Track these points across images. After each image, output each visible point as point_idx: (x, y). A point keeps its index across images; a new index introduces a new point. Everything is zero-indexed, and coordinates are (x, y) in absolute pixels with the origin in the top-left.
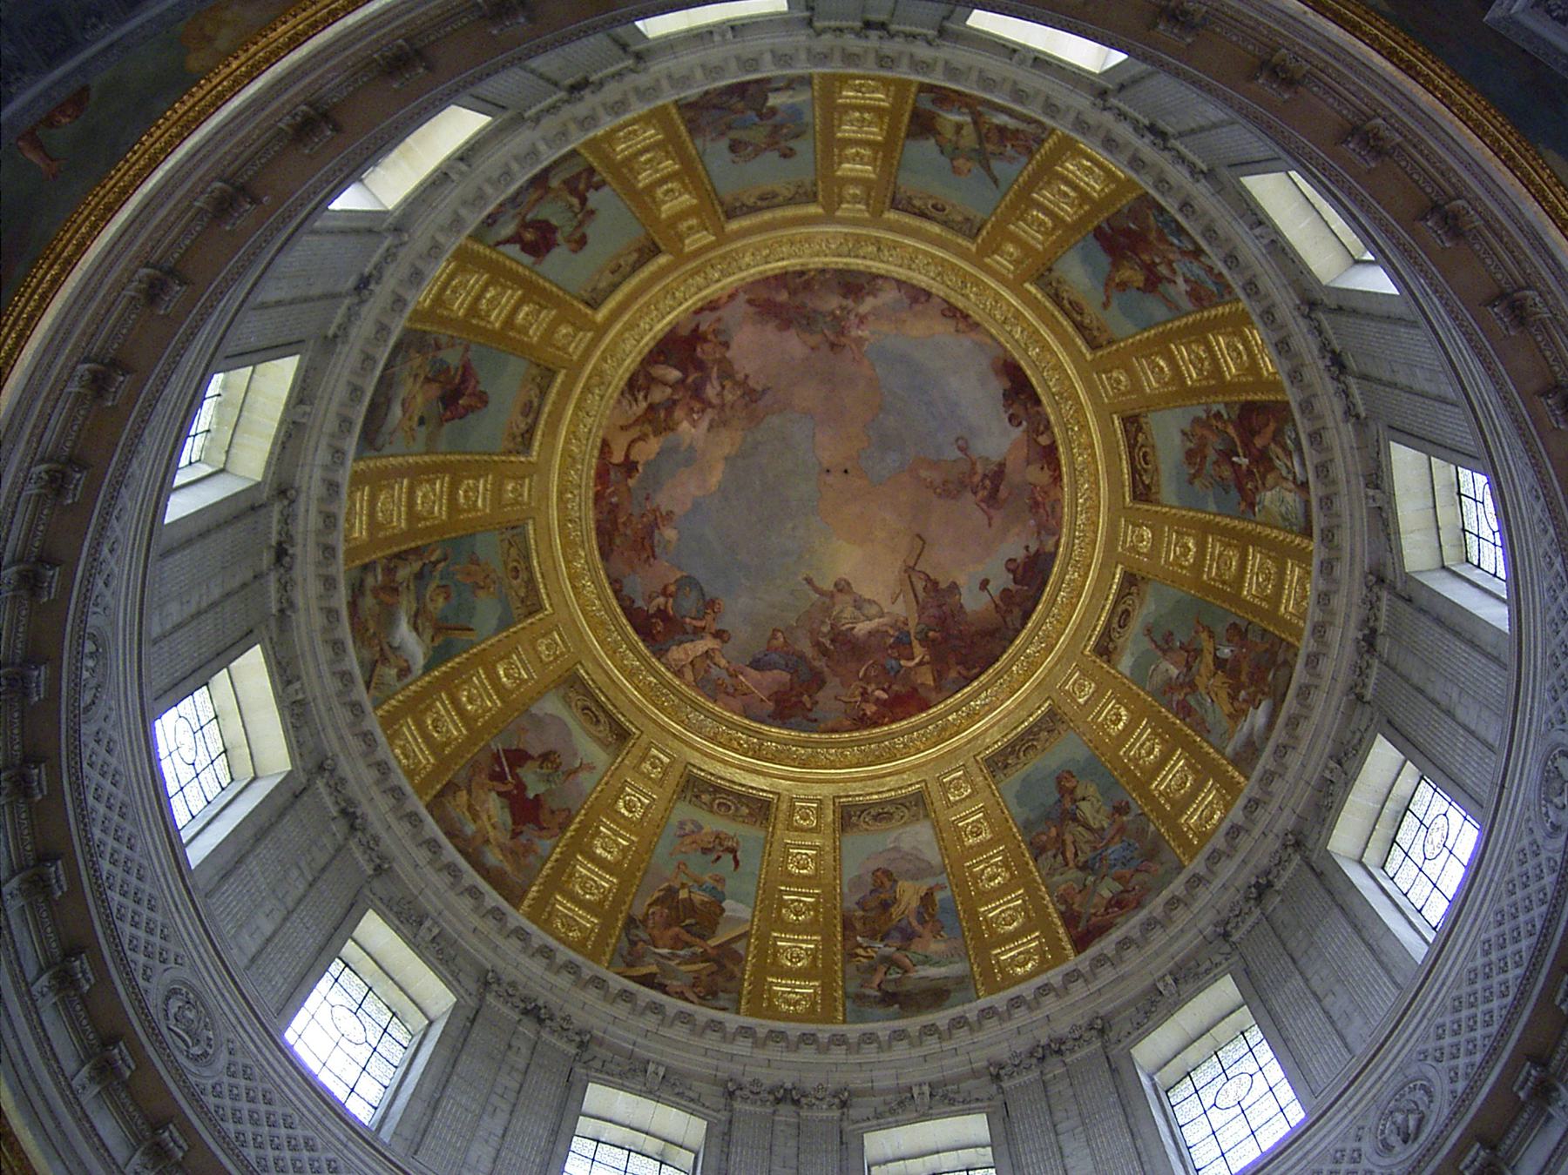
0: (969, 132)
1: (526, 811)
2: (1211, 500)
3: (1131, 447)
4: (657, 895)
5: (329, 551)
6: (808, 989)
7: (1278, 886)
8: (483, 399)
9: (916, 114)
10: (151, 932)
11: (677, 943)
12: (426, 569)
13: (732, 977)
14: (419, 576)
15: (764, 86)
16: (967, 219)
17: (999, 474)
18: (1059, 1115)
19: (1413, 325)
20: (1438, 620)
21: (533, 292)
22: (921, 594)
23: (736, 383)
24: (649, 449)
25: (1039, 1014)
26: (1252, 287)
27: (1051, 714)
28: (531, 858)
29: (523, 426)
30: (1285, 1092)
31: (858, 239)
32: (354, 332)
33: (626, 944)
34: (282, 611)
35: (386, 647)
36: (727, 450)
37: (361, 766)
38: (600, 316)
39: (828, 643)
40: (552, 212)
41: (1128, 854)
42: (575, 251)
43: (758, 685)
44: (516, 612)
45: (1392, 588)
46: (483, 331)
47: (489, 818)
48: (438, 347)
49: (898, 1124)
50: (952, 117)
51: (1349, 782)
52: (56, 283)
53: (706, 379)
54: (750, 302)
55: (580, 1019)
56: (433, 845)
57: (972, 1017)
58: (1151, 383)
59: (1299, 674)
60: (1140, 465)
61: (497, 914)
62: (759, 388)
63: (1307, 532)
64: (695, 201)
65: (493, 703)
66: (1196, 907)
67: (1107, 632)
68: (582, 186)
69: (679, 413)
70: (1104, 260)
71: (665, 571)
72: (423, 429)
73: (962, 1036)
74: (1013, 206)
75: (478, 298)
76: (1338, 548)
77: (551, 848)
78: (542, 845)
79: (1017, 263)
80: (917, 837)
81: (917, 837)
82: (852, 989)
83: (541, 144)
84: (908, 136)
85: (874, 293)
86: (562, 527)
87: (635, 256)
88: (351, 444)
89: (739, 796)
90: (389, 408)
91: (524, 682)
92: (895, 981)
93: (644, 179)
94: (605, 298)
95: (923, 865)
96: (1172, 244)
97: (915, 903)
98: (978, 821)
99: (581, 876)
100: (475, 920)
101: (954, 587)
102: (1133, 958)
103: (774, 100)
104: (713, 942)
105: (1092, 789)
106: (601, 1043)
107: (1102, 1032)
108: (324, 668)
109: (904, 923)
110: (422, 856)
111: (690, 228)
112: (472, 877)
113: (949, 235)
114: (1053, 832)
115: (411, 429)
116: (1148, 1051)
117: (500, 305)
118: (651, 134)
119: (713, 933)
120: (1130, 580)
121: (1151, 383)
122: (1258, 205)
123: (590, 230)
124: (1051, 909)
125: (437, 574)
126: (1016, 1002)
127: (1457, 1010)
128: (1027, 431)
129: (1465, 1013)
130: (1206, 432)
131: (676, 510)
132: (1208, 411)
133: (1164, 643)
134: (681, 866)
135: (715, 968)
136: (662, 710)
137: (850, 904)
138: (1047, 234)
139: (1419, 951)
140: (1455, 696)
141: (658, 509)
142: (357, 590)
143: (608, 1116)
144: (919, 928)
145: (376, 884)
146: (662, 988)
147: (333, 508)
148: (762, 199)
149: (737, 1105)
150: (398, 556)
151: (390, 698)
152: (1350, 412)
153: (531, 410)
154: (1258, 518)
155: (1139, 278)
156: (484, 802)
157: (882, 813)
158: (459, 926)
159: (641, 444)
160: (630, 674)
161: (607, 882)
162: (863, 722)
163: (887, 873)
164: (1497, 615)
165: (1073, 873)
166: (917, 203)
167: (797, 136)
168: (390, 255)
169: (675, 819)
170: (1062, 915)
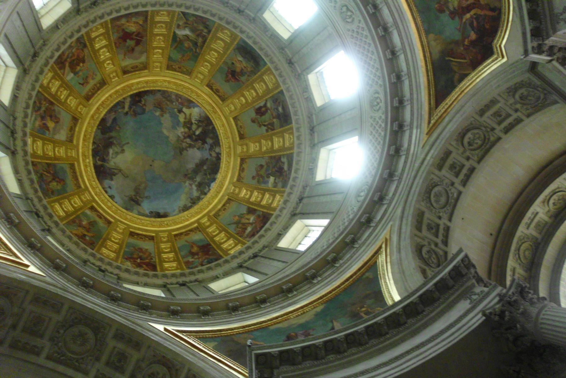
0: (247, 221)
1: (126, 36)
3: (145, 236)
8: (227, 81)
11: (73, 55)
14: (196, 44)
16: (219, 215)
17: (138, 203)
24: (181, 118)
27: (79, 187)
29: (214, 88)
31: (222, 188)
33: (83, 41)
39: (111, 140)
40: (267, 117)
53: (192, 140)
54: (207, 159)
55: (85, 15)
60: (141, 236)
67: (96, 211)
69: (186, 130)
70: (201, 244)
71: (149, 108)
72: (230, 63)
75: (256, 91)
79: (204, 224)
80: (62, 136)
84: (249, 208)
85: (197, 190)
87: (242, 133)
89: (93, 95)
90: (242, 57)
91: (154, 55)
93: (263, 142)
101: (112, 180)
103: (272, 179)
104: (67, 64)
105: (59, 187)
106: (74, 16)
108: (202, 6)
112: (123, 12)
114: (52, 172)
117: (250, 95)
120: (109, 223)
123: (255, 126)
124: (35, 160)
133: (92, 224)
135: (63, 61)
136: (124, 87)
137: (56, 108)
147: (238, 30)
148: (243, 169)
150: (204, 42)
153: (216, 92)
157: (72, 129)
159: (184, 116)
160: (138, 83)
167: (258, 182)
169: (98, 74)
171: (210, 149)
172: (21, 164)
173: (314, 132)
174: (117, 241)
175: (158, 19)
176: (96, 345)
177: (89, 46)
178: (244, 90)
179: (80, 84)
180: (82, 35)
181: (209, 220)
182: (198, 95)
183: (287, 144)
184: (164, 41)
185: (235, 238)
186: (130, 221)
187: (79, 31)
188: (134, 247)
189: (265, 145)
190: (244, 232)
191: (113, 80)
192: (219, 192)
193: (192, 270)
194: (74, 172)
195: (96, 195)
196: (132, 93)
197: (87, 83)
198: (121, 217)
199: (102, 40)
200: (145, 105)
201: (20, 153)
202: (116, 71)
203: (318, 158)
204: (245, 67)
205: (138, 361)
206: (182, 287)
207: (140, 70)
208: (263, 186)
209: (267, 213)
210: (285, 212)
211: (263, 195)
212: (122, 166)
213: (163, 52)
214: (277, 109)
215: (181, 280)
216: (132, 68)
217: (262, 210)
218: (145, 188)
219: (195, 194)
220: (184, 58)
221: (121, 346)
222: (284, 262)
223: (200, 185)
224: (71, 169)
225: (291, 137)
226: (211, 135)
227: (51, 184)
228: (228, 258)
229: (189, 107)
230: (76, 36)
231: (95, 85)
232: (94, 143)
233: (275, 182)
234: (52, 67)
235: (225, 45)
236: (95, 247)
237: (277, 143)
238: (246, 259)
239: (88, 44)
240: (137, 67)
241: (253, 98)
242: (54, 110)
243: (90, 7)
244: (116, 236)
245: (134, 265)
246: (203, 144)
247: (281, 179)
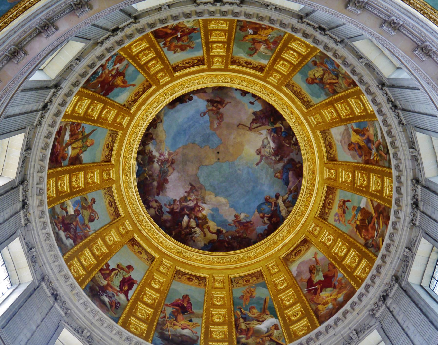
0: (74, 145)
1: (328, 282)
2: (197, 41)
4: (358, 233)
8: (186, 297)
9: (71, 164)
11: (373, 228)
12: (243, 316)
13: (384, 209)
14: (245, 319)
17: (211, 102)
21: (147, 283)
22: (258, 125)
23: (189, 195)
25: (383, 104)
27: (287, 86)
28: (343, 281)
29: (196, 281)
33: (372, 249)
35: (267, 334)
36: (213, 196)
39: (278, 157)
40: (116, 281)
41: (329, 62)
42: (133, 269)
43: (294, 183)
44: (262, 281)
47: (328, 297)
48: (165, 317)
49: (422, 164)
50: (70, 152)
53: (187, 207)
54: (158, 194)
55: (388, 279)
62: (190, 187)
64: (113, 230)
67: (255, 68)
68: (108, 272)
69: (200, 215)
70: (116, 90)
71: (255, 217)
72: (193, 320)
77: (340, 274)
79: (124, 117)
80: (337, 133)
82: (387, 165)
85: (151, 153)
87: (135, 247)
89: (326, 198)
93: (105, 250)
94: (151, 255)
95: (345, 132)
96: (102, 73)
97: (358, 137)
98: (328, 112)
99: (350, 263)
100: (355, 313)
101: (254, 113)
103: (71, 211)
109: (366, 142)
111: (123, 229)
112: (347, 306)
113: (117, 141)
114: (328, 86)
115: (193, 325)
119: (370, 213)
120: (234, 62)
121: (159, 66)
122: (63, 70)
123: (124, 264)
124: (353, 90)
125: (245, 312)
130: (172, 47)
131: (234, 214)
132: (164, 47)
133: (253, 51)
135: (381, 215)
137: (360, 160)
141: (233, 221)
143: (422, 273)
148: (111, 206)
150: (237, 328)
151: (283, 334)
153: (191, 278)
154: (198, 27)
155: (119, 78)
156: (323, 298)
157: (330, 146)
158: (355, 321)
159: (211, 229)
160: (284, 238)
163: (350, 145)
165: (340, 81)
166: (107, 153)
167: (86, 200)
171: (161, 207)
172: (368, 77)
173: (52, 294)
174: (215, 45)
175: (305, 321)
177: (361, 247)
178: (160, 296)
179: (348, 201)
180: (377, 256)
181: (121, 124)
183: (75, 262)
184: (282, 301)
186: (211, 77)
187: (384, 257)
188: (190, 47)
189: (100, 247)
190: (71, 131)
191: (313, 225)
192: (125, 162)
193: (112, 53)
194: (302, 99)
195: (265, 87)
196: (285, 222)
197: (340, 207)
198: (224, 76)
200: (262, 218)
201: (374, 88)
202: (316, 237)
203: (30, 266)
204: (174, 325)
206: (115, 27)
207: (291, 253)
209: (55, 168)
210: (36, 180)
211: (71, 187)
213: (276, 287)
214: (110, 297)
215: (120, 35)
216: (300, 250)
217: (63, 168)
219: (151, 147)
220: (249, 295)
222: (8, 117)
223: (151, 159)
224: (308, 101)
225: (75, 274)
226: (168, 225)
227: (322, 72)
228: (76, 90)
229: (211, 242)
230: (383, 250)
231: (331, 209)
232: (296, 143)
233: (66, 210)
234: (390, 203)
235: (211, 337)
236: (237, 25)
237: (88, 258)
238: (54, 100)
239: (365, 250)
240: (296, 255)
241: (145, 294)
242: (360, 156)
243: (386, 291)
244: (218, 51)
245: (182, 26)
246: (172, 210)
247: (60, 217)
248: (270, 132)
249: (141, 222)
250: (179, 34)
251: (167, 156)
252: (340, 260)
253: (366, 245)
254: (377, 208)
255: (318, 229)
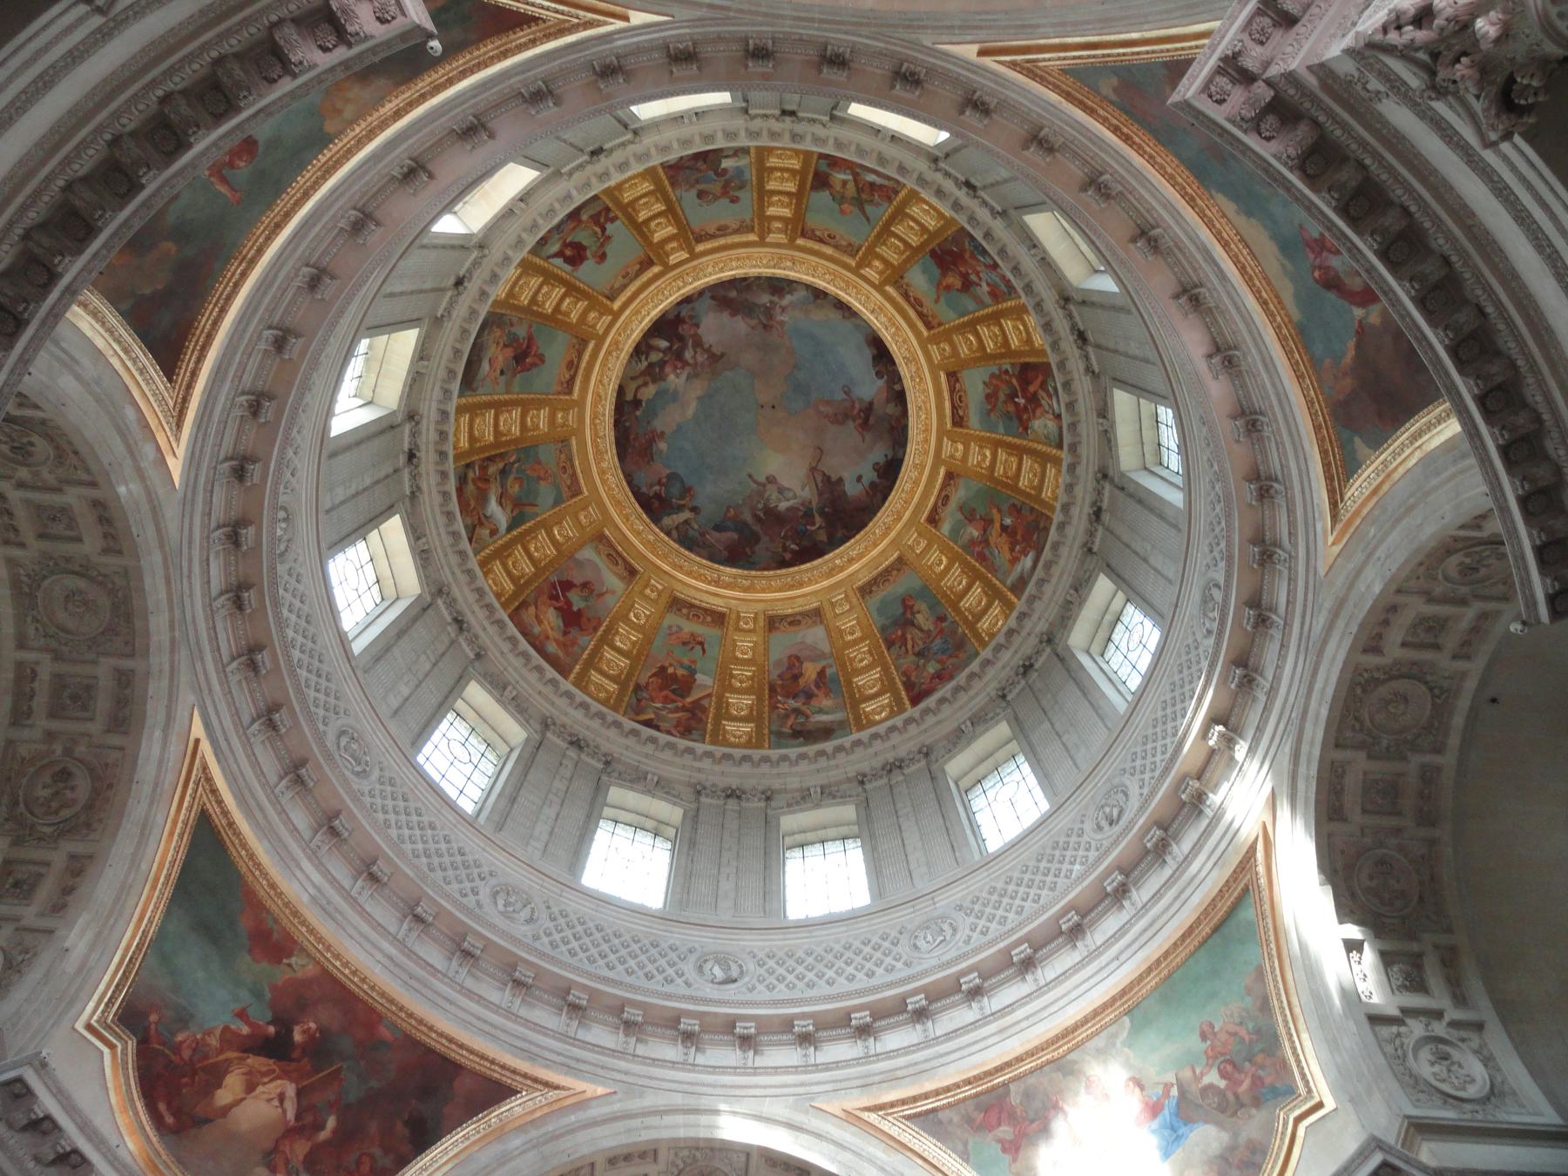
1: (572, 619)
3: (952, 391)
5: (442, 455)
6: (747, 728)
7: (1037, 666)
8: (541, 359)
9: (817, 174)
10: (327, 695)
11: (666, 700)
13: (701, 720)
14: (504, 472)
15: (718, 154)
17: (869, 409)
18: (899, 805)
19: (1129, 312)
20: (1140, 502)
21: (572, 289)
24: (648, 392)
25: (888, 744)
26: (1028, 288)
27: (900, 560)
28: (576, 648)
30: (1038, 792)
32: (454, 313)
34: (413, 493)
36: (699, 393)
37: (467, 591)
38: (616, 305)
40: (583, 236)
45: (1112, 481)
46: (540, 315)
49: (802, 810)
50: (839, 176)
51: (1082, 602)
52: (244, 275)
54: (713, 298)
55: (606, 747)
56: (512, 639)
57: (848, 745)
58: (964, 351)
59: (1053, 534)
61: (553, 682)
63: (1060, 446)
65: (551, 551)
66: (986, 679)
67: (935, 509)
69: (668, 369)
70: (936, 271)
73: (841, 757)
74: (879, 236)
76: (1079, 456)
77: (588, 642)
78: (583, 640)
79: (881, 273)
80: (815, 636)
81: (815, 636)
82: (774, 728)
83: (576, 190)
85: (790, 292)
86: (594, 442)
88: (455, 387)
89: (706, 610)
92: (802, 724)
97: (814, 676)
100: (540, 687)
101: (840, 480)
102: (946, 710)
104: (689, 700)
107: (927, 755)
108: (442, 530)
110: (506, 647)
112: (537, 659)
113: (837, 255)
116: (955, 766)
117: (552, 298)
118: (647, 186)
120: (950, 476)
123: (609, 249)
126: (875, 736)
127: (1145, 744)
128: (887, 382)
129: (1149, 746)
133: (969, 514)
134: (669, 653)
138: (901, 253)
139: (1122, 706)
140: (1149, 548)
142: (462, 480)
144: (816, 691)
145: (477, 664)
146: (657, 728)
147: (445, 428)
149: (703, 799)
150: (490, 459)
152: (1089, 370)
153: (572, 366)
155: (958, 283)
157: (794, 621)
159: (643, 389)
160: (638, 533)
161: (624, 663)
162: (783, 564)
163: (797, 658)
164: (1176, 498)
165: (911, 658)
167: (740, 188)
168: (476, 264)
170: (904, 684)
174: (988, 453)
176: (1402, 676)
181: (869, 265)
182: (598, 398)
185: (906, 202)
186: (927, 430)
190: (881, 186)
195: (899, 518)
198: (926, 453)
199: (609, 661)
200: (659, 482)
205: (1431, 599)
207: (611, 546)
208: (751, 176)
212: (802, 471)
218: (828, 403)
221: (1395, 635)
227: (925, 628)
240: (609, 555)
242: (780, 677)
244: (978, 457)
248: (806, 504)
249: (680, 276)
250: (1022, 401)
251: (780, 318)
252: (606, 640)
253: (638, 687)
254: (696, 703)
255: (654, 595)
